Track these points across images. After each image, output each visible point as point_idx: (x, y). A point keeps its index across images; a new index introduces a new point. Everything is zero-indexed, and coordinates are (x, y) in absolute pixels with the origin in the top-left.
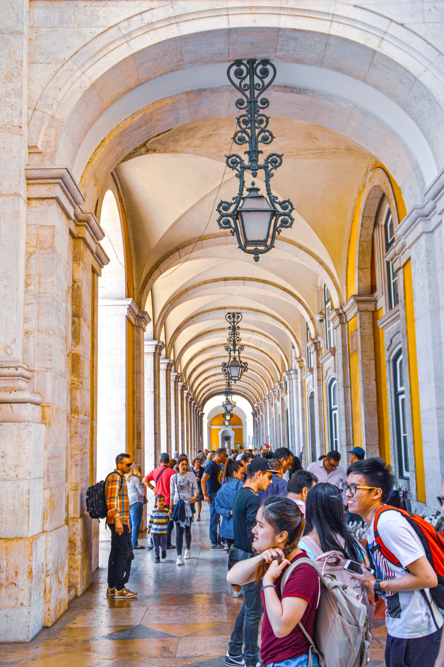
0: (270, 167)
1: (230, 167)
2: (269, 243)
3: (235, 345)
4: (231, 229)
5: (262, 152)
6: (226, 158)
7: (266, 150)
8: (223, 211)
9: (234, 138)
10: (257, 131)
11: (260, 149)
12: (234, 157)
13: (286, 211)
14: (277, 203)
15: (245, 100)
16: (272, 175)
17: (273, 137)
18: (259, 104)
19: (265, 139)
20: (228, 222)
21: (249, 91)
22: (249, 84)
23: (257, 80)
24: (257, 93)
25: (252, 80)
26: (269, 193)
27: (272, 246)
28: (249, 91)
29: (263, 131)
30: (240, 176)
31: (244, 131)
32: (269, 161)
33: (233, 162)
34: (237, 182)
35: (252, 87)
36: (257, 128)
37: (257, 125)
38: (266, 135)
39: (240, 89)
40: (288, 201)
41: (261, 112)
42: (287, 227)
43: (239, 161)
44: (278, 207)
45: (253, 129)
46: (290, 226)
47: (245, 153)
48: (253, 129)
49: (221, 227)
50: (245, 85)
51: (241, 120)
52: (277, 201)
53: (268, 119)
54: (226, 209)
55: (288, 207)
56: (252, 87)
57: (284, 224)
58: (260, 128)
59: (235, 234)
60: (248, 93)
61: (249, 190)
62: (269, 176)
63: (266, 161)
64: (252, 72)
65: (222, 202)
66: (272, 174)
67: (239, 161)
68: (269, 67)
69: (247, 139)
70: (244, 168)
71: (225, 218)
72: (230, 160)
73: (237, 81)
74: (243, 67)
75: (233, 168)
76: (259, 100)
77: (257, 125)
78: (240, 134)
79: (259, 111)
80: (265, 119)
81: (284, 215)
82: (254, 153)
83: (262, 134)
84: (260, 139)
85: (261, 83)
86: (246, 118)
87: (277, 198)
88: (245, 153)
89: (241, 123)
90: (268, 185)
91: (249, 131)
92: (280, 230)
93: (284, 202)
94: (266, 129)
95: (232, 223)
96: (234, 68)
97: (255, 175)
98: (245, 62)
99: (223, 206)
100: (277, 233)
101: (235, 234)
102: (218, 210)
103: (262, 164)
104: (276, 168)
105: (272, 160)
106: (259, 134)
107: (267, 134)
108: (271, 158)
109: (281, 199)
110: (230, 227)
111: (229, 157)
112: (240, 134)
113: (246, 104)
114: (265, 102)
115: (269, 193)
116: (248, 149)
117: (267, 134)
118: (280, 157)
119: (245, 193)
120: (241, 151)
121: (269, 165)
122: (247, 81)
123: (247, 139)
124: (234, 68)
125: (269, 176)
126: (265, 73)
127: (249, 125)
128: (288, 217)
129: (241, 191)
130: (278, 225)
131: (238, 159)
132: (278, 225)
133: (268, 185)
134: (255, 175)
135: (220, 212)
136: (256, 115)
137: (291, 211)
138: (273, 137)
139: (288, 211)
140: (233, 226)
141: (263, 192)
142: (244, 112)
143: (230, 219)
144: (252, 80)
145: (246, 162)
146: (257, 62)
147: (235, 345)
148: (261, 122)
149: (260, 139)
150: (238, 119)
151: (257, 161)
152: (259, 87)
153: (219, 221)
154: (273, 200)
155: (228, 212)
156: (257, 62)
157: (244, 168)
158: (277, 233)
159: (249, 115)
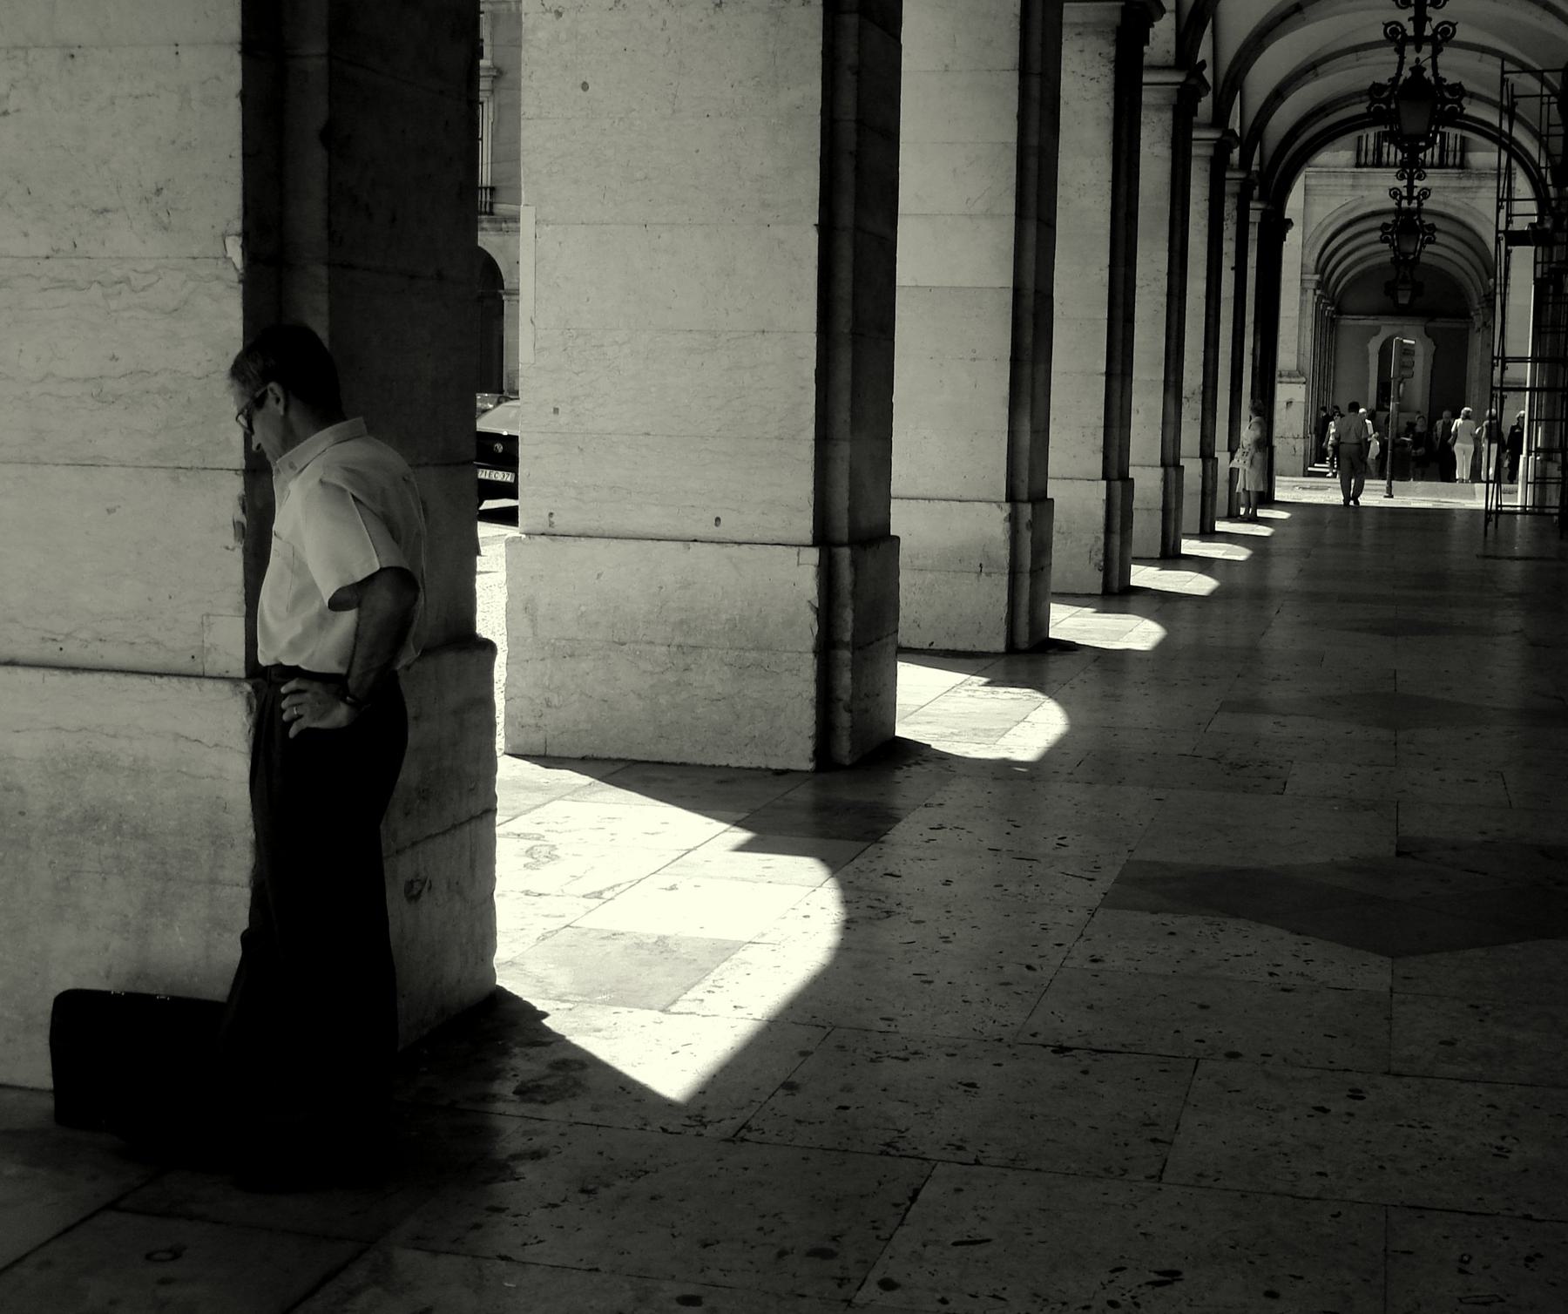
26: (1435, 73)
63: (1435, 31)
70: (1407, 40)
90: (1435, 66)
97: (1418, 50)
111: (1387, 25)
118: (1453, 25)
119: (1406, 73)
120: (1405, 17)
133: (1435, 66)
134: (1418, 50)
141: (1428, 74)
154: (1440, 80)
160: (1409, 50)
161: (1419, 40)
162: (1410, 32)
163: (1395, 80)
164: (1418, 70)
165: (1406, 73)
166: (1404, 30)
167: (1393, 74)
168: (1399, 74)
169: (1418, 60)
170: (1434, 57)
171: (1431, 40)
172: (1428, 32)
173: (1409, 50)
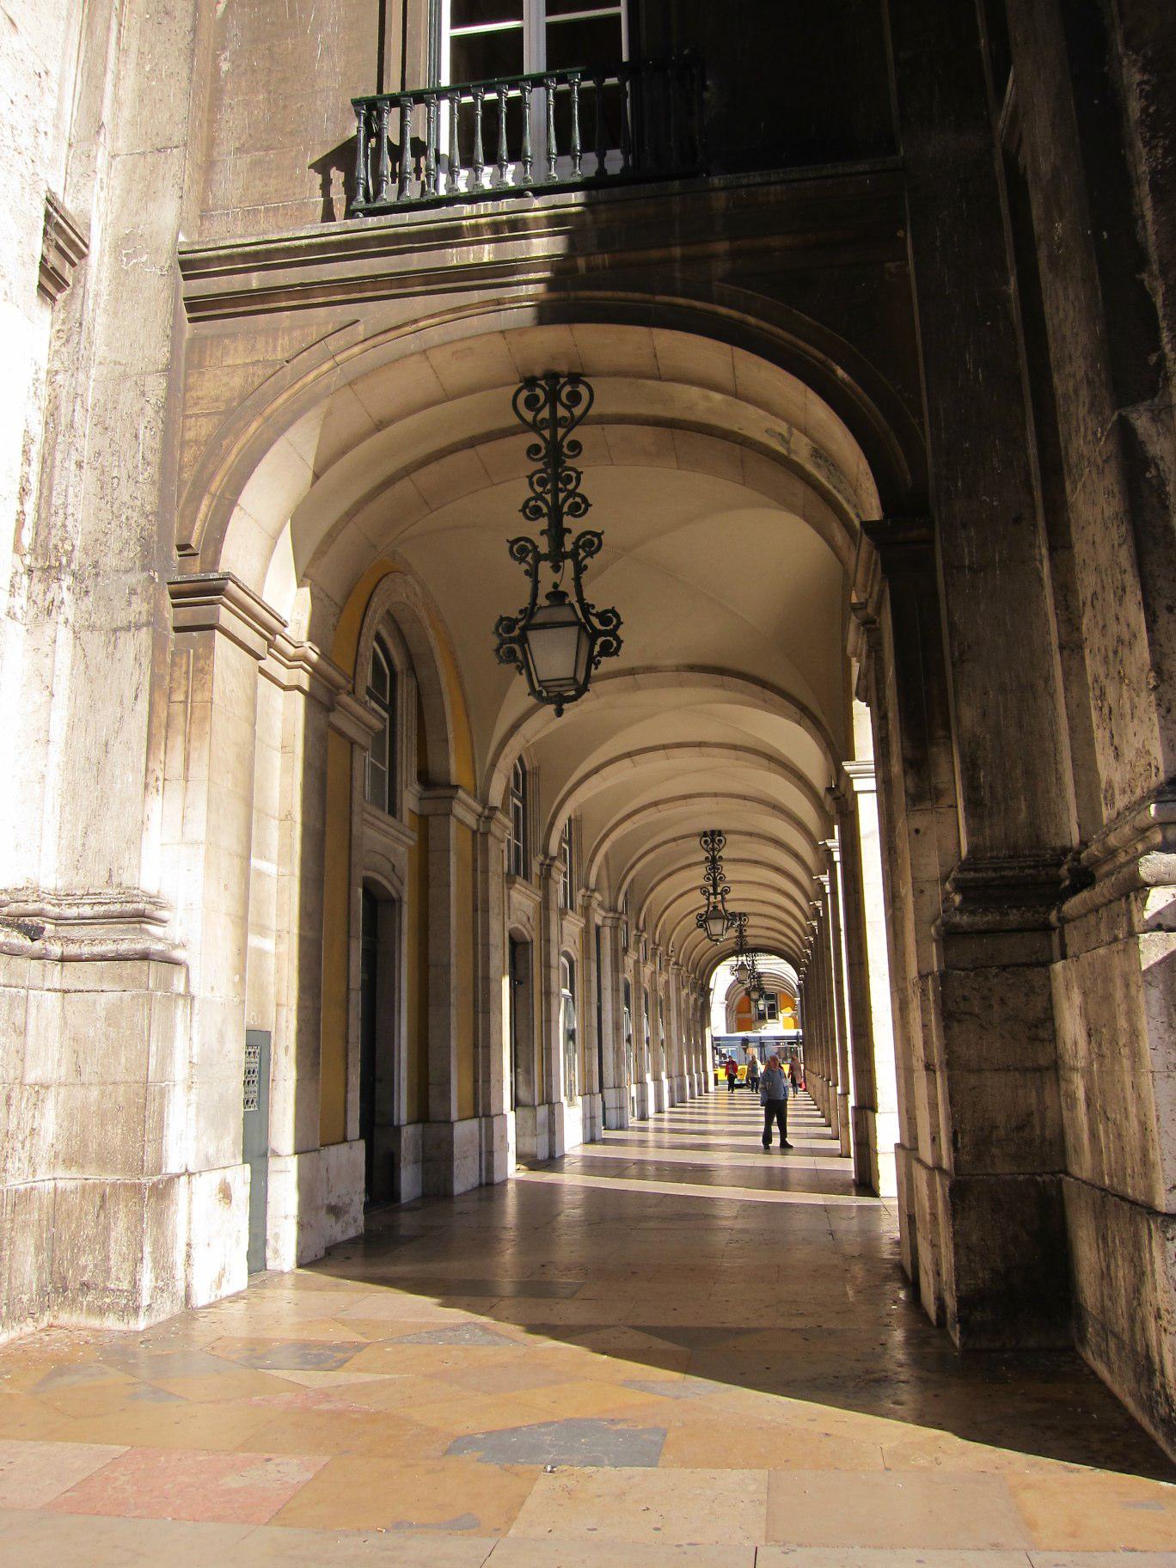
0: (582, 554)
1: (515, 558)
3: (715, 886)
9: (523, 510)
10: (562, 496)
11: (565, 525)
15: (542, 444)
16: (586, 567)
17: (588, 505)
18: (565, 450)
19: (576, 511)
20: (512, 652)
24: (561, 431)
25: (553, 411)
26: (581, 599)
30: (533, 573)
33: (521, 549)
34: (528, 581)
35: (555, 422)
36: (561, 490)
39: (535, 427)
40: (613, 611)
41: (569, 463)
44: (595, 622)
46: (616, 653)
47: (542, 533)
49: (501, 661)
51: (535, 479)
53: (579, 474)
54: (509, 629)
56: (555, 422)
57: (607, 650)
60: (547, 433)
61: (548, 596)
62: (580, 569)
63: (576, 544)
64: (553, 398)
65: (502, 619)
69: (545, 510)
70: (539, 558)
73: (529, 416)
74: (539, 391)
75: (522, 560)
76: (565, 443)
80: (574, 475)
82: (557, 532)
83: (571, 501)
84: (565, 509)
85: (567, 414)
87: (593, 607)
88: (542, 533)
91: (548, 497)
93: (607, 611)
95: (519, 654)
97: (556, 568)
98: (542, 383)
99: (506, 624)
104: (590, 554)
106: (565, 500)
109: (599, 609)
110: (515, 660)
112: (532, 503)
113: (543, 452)
114: (576, 446)
115: (581, 599)
117: (578, 500)
118: (598, 535)
119: (542, 601)
120: (536, 530)
122: (545, 413)
123: (545, 510)
124: (525, 394)
125: (580, 569)
126: (575, 398)
129: (535, 595)
137: (617, 627)
138: (588, 505)
142: (540, 465)
143: (516, 647)
144: (553, 411)
146: (562, 381)
147: (715, 886)
148: (569, 479)
149: (565, 509)
150: (530, 478)
151: (562, 544)
153: (497, 651)
154: (586, 608)
156: (562, 381)
157: (539, 558)
160: (545, 567)
161: (715, 893)
162: (544, 546)
163: (530, 612)
164: (557, 597)
166: (535, 547)
167: (525, 602)
170: (577, 579)
171: (574, 555)
172: (568, 546)
173: (712, 899)
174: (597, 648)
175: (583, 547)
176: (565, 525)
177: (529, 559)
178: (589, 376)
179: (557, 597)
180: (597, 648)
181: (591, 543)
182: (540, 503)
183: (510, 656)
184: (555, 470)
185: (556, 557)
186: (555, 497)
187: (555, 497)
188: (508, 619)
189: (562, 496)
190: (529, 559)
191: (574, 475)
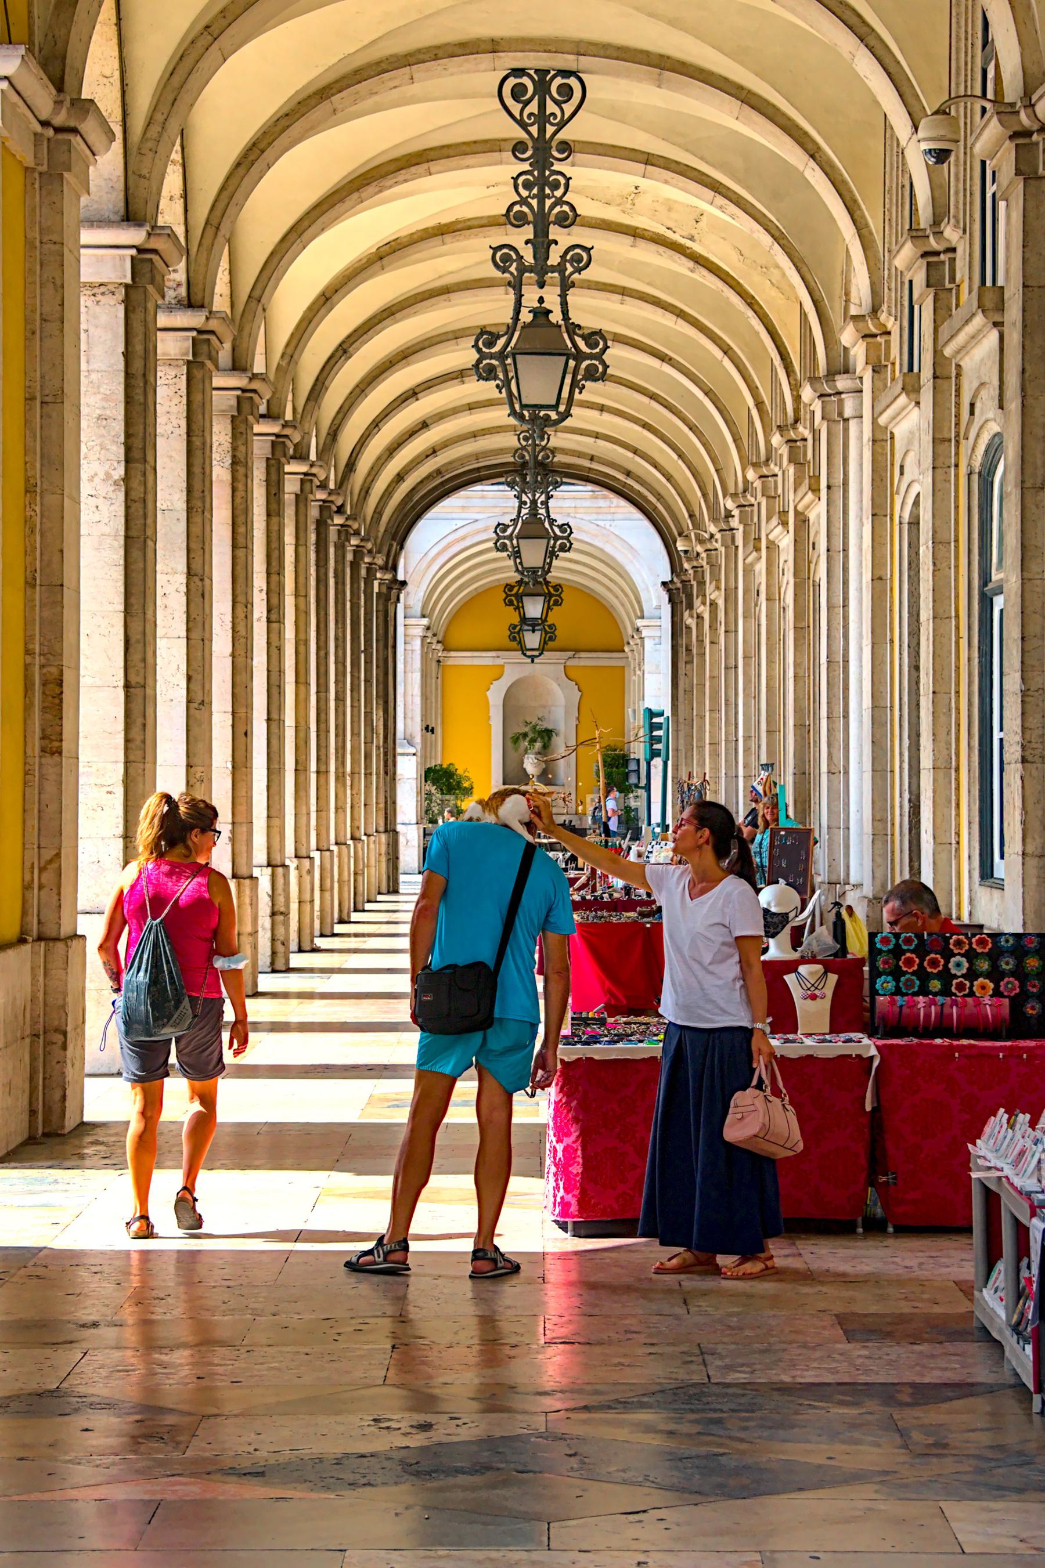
0: (570, 269)
2: (562, 408)
4: (498, 382)
5: (556, 243)
6: (491, 251)
7: (563, 238)
8: (484, 350)
10: (548, 203)
11: (551, 237)
12: (505, 251)
13: (594, 351)
14: (579, 336)
15: (530, 144)
21: (536, 126)
22: (536, 112)
23: (551, 107)
24: (550, 130)
25: (542, 106)
27: (567, 414)
28: (536, 126)
29: (559, 202)
30: (517, 286)
31: (523, 201)
32: (568, 257)
35: (542, 118)
36: (549, 198)
37: (547, 191)
38: (565, 212)
41: (557, 167)
42: (596, 380)
43: (514, 257)
45: (542, 198)
47: (527, 242)
48: (542, 198)
49: (480, 378)
50: (531, 115)
52: (579, 332)
54: (490, 344)
55: (597, 345)
56: (542, 118)
57: (592, 375)
58: (553, 196)
59: (504, 390)
60: (534, 130)
62: (566, 286)
63: (563, 257)
66: (573, 282)
67: (514, 257)
68: (573, 82)
69: (531, 218)
70: (522, 269)
71: (488, 361)
72: (499, 254)
73: (515, 108)
74: (526, 80)
75: (504, 270)
76: (554, 144)
77: (547, 191)
78: (517, 208)
79: (552, 164)
80: (563, 181)
81: (591, 357)
82: (542, 244)
83: (558, 209)
84: (552, 218)
86: (529, 177)
88: (527, 242)
89: (520, 187)
90: (564, 305)
91: (534, 203)
92: (584, 387)
94: (564, 199)
96: (512, 82)
98: (532, 72)
100: (577, 390)
101: (504, 390)
102: (476, 346)
103: (556, 264)
104: (579, 271)
105: (572, 256)
106: (553, 206)
107: (566, 208)
108: (571, 253)
110: (496, 378)
111: (495, 250)
112: (517, 208)
114: (566, 147)
116: (531, 237)
117: (566, 208)
118: (588, 250)
119: (526, 317)
120: (520, 238)
121: (568, 265)
122: (533, 107)
123: (531, 218)
124: (512, 82)
125: (566, 286)
126: (566, 92)
127: (535, 191)
128: (597, 363)
130: (579, 377)
131: (512, 253)
132: (579, 377)
133: (564, 305)
135: (479, 351)
136: (547, 173)
139: (597, 350)
140: (501, 376)
141: (556, 317)
142: (526, 166)
144: (542, 106)
145: (529, 258)
148: (556, 186)
149: (552, 218)
150: (515, 179)
152: (555, 118)
154: (573, 329)
155: (493, 350)
156: (552, 73)
158: (577, 390)
159: (536, 173)
162: (528, 255)
164: (541, 313)
165: (526, 317)
168: (516, 318)
169: (541, 300)
170: (563, 296)
171: (560, 268)
172: (554, 259)
174: (582, 372)
175: (571, 261)
176: (551, 237)
177: (513, 269)
178: (583, 72)
179: (541, 313)
180: (582, 372)
181: (580, 259)
182: (525, 209)
183: (489, 374)
184: (542, 173)
185: (541, 269)
186: (541, 204)
187: (541, 204)
188: (490, 333)
189: (548, 203)
190: (513, 269)
191: (563, 181)
